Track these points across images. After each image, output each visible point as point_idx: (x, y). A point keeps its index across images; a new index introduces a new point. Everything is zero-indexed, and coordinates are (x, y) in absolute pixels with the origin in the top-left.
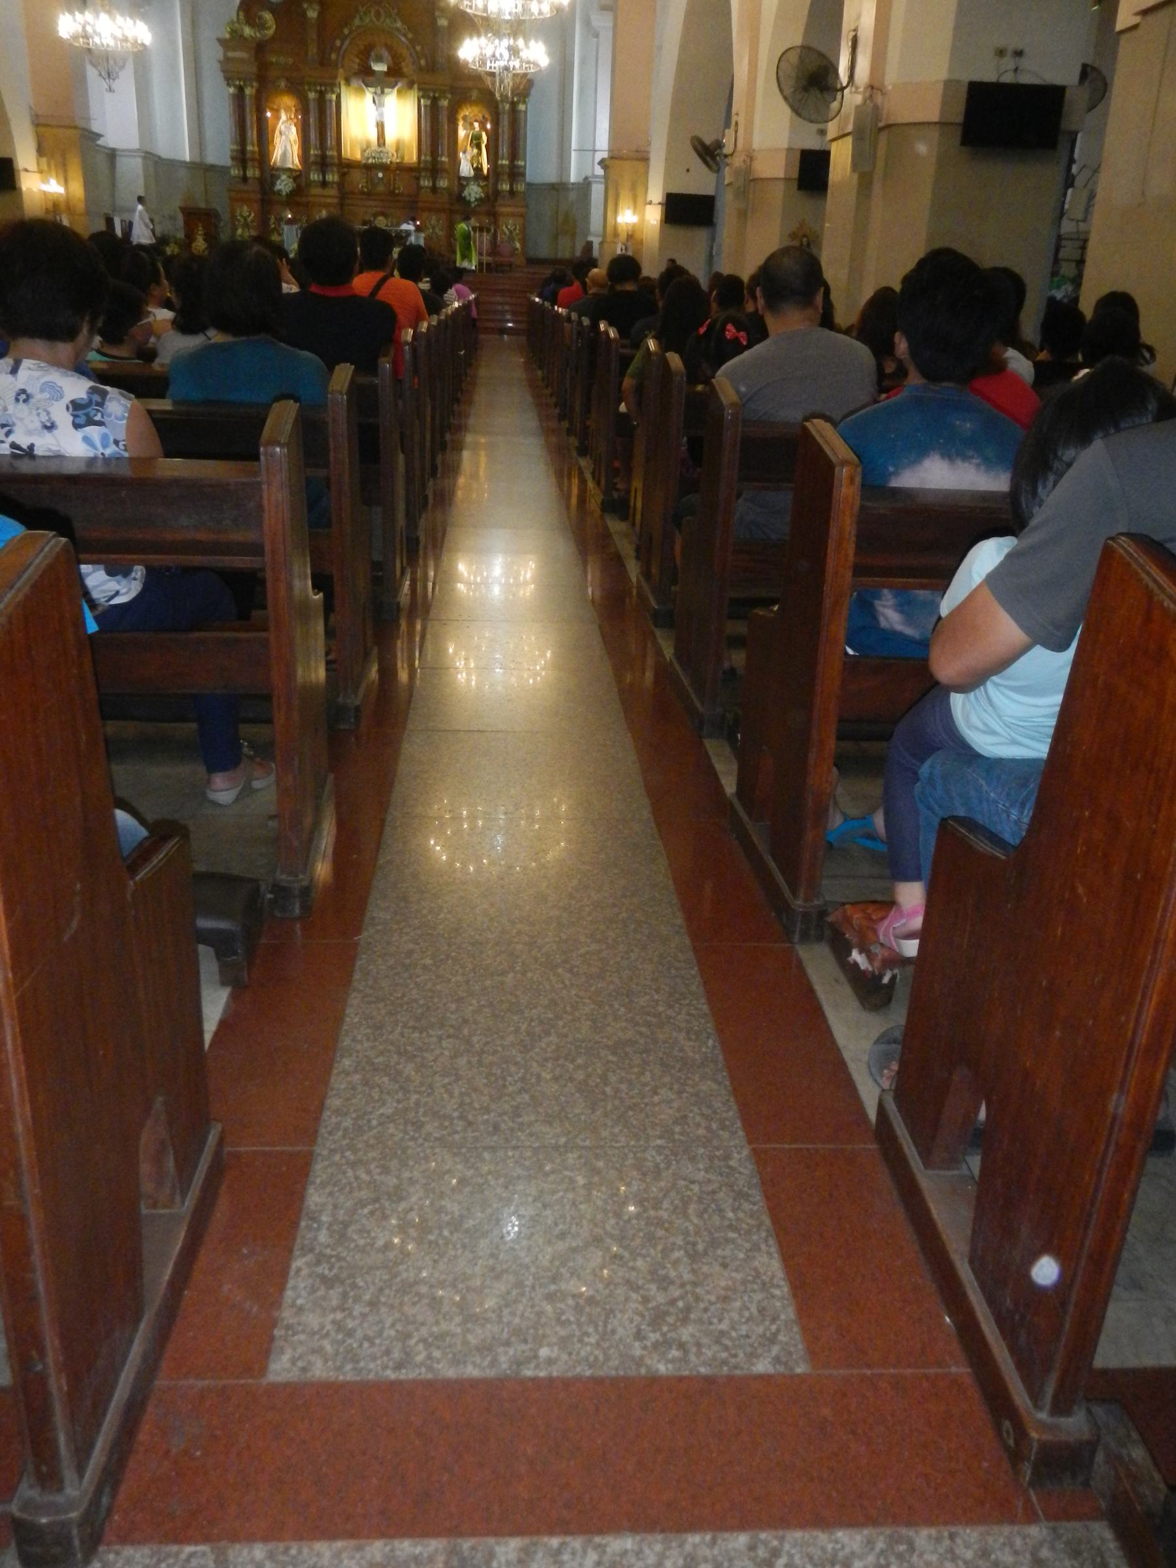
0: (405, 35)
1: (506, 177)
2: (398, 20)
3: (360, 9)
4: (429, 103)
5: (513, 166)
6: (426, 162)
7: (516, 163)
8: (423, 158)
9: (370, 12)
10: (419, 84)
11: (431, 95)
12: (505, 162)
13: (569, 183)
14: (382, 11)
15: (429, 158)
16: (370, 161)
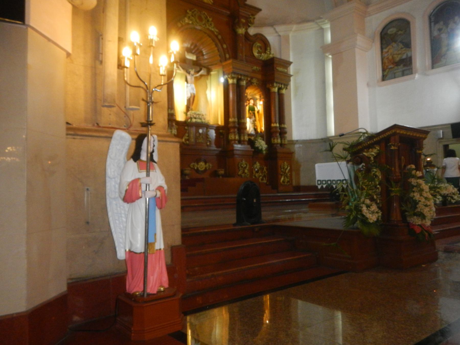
0: (217, 36)
1: (278, 135)
2: (213, 25)
3: (188, 11)
4: (235, 81)
5: (280, 128)
6: (234, 122)
7: (283, 126)
8: (231, 120)
9: (195, 15)
10: (233, 68)
11: (240, 77)
12: (278, 125)
13: (293, 141)
14: (203, 17)
15: (236, 120)
16: (194, 120)
